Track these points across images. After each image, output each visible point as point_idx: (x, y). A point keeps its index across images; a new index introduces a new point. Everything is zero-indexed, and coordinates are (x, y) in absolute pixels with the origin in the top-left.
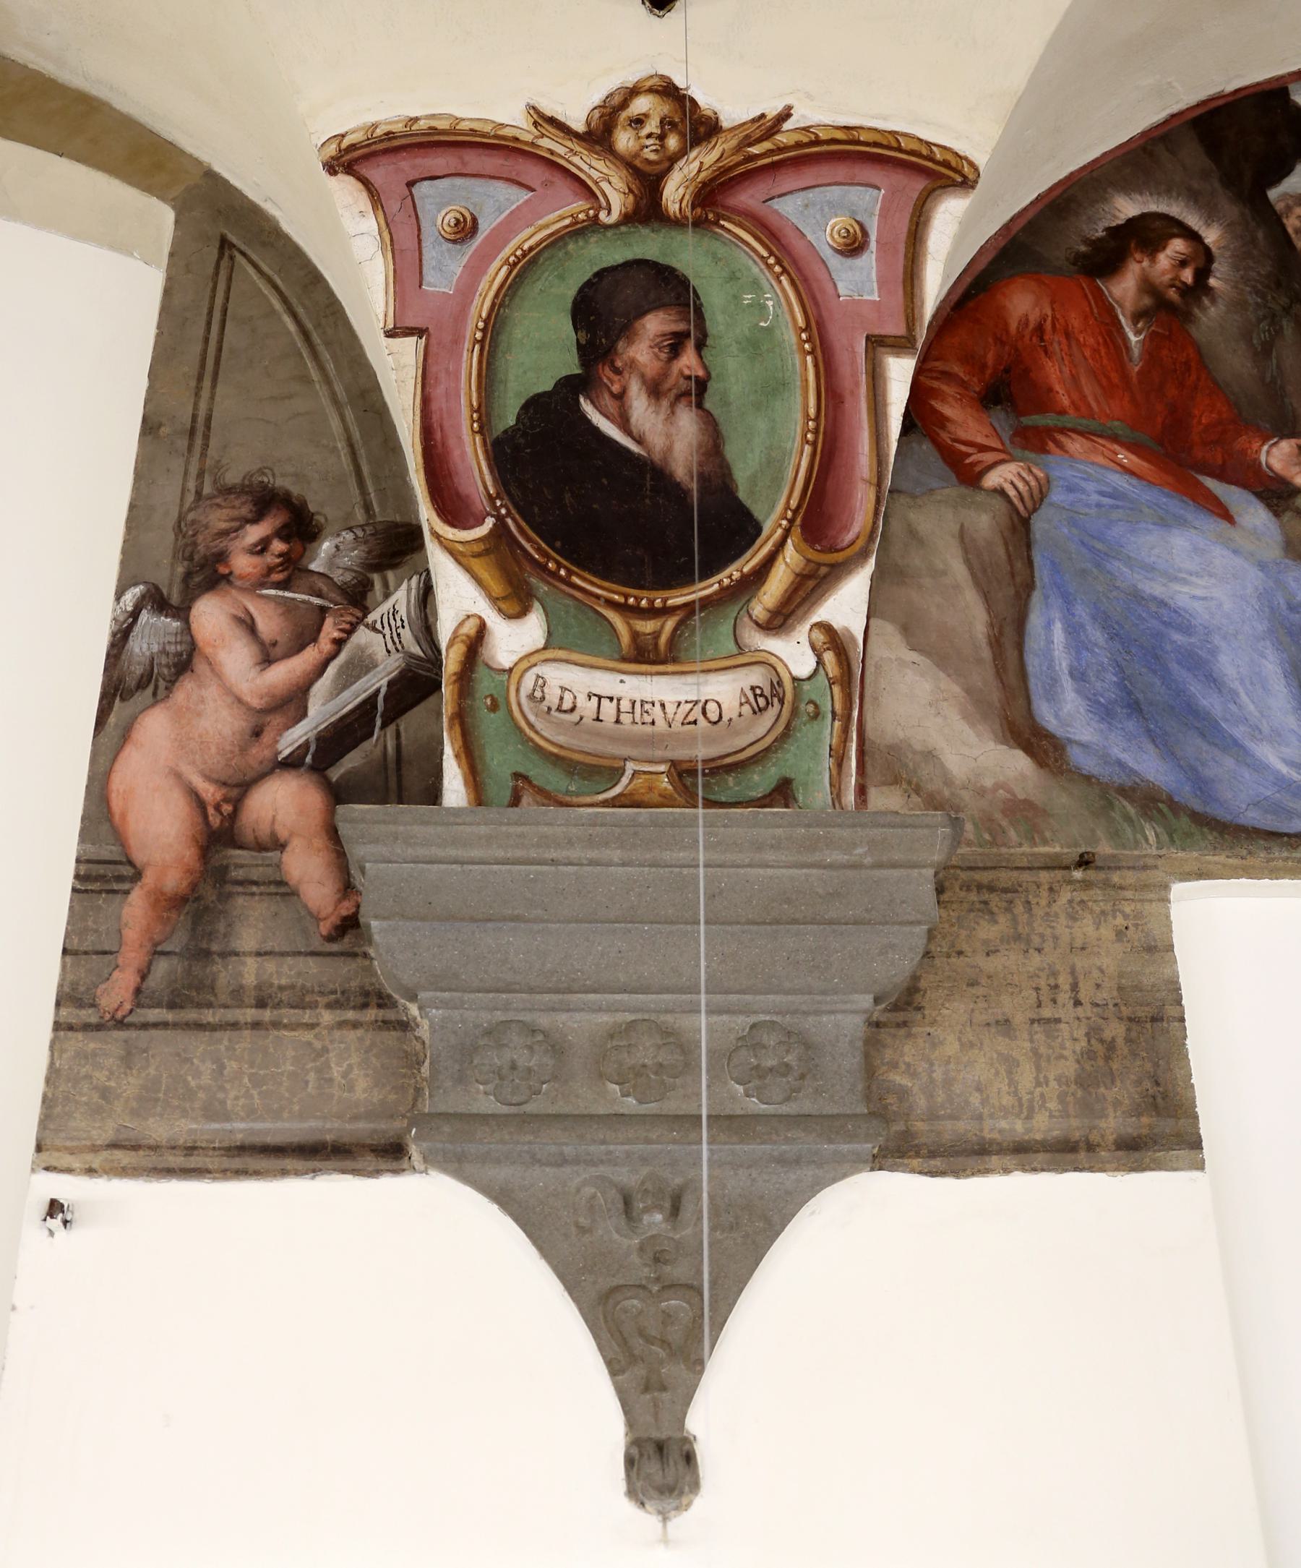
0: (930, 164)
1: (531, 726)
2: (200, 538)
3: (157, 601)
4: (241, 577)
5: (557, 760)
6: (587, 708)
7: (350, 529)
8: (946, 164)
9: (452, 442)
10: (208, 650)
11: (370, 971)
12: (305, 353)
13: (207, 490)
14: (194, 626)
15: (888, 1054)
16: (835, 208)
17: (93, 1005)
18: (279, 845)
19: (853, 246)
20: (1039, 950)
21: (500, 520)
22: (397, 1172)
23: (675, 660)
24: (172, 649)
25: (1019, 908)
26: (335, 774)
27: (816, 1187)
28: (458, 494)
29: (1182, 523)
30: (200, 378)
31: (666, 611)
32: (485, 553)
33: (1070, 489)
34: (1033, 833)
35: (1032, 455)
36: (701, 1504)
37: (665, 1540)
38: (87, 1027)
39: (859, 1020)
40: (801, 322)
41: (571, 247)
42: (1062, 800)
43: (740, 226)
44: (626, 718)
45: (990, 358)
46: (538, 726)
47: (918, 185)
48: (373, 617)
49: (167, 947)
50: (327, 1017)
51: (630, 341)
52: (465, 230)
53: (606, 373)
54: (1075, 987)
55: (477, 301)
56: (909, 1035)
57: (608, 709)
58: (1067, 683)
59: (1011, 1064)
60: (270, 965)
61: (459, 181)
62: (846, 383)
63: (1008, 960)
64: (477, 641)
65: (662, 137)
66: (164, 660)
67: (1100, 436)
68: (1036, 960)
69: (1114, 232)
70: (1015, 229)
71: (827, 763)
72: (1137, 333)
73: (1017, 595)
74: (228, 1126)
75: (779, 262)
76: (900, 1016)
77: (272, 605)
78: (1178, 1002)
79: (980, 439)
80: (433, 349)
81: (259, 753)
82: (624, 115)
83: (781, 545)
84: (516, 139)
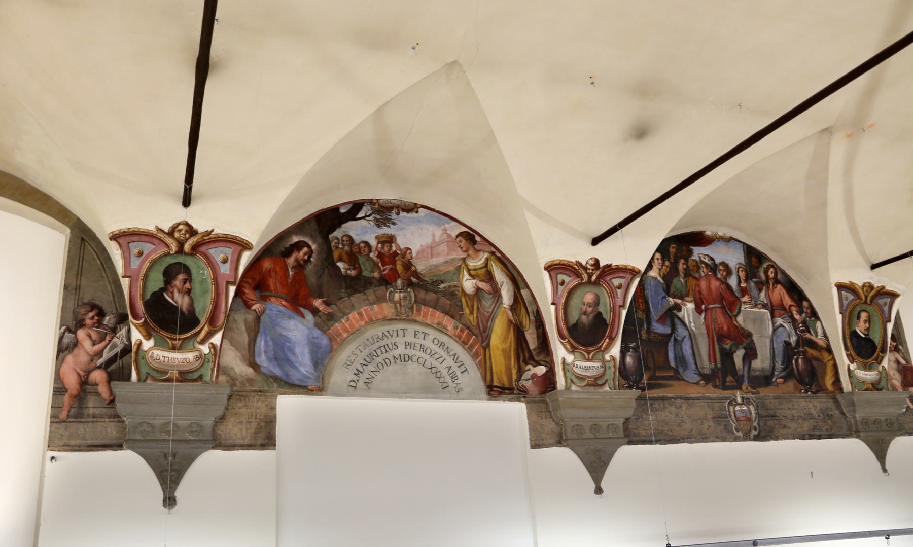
0: (243, 244)
1: (150, 363)
2: (78, 315)
3: (69, 330)
4: (88, 325)
5: (155, 370)
6: (162, 359)
7: (112, 314)
8: (246, 244)
9: (136, 301)
10: (81, 342)
11: (116, 411)
12: (102, 270)
13: (80, 304)
14: (78, 336)
15: (218, 428)
16: (222, 252)
17: (58, 418)
18: (97, 385)
19: (225, 261)
20: (250, 408)
21: (146, 319)
22: (121, 450)
23: (181, 350)
24: (73, 341)
25: (247, 400)
26: (109, 370)
27: (201, 453)
28: (136, 312)
29: (293, 318)
30: (77, 275)
31: (179, 339)
32: (142, 326)
33: (271, 310)
34: (251, 385)
35: (262, 302)
36: (176, 507)
37: (169, 513)
38: (57, 422)
39: (212, 422)
40: (212, 277)
41: (163, 259)
42: (258, 378)
43: (200, 255)
44: (170, 361)
45: (257, 278)
46: (152, 363)
47: (240, 248)
48: (117, 335)
49: (74, 406)
50: (107, 420)
51: (175, 280)
52: (140, 254)
53: (170, 287)
54: (256, 415)
55: (142, 270)
56: (222, 424)
57: (166, 359)
58: (263, 354)
59: (241, 430)
60: (95, 410)
61: (139, 243)
62: (221, 292)
63: (244, 410)
64: (140, 345)
65: (185, 234)
66: (71, 344)
67: (279, 297)
68: (249, 410)
69: (292, 246)
70: (268, 245)
71: (210, 371)
72: (292, 272)
73: (255, 334)
74: (87, 441)
75: (208, 264)
76: (221, 421)
77: (95, 332)
78: (276, 418)
79: (252, 298)
80: (132, 281)
81: (92, 365)
82: (177, 229)
83: (204, 326)
84: (152, 233)
